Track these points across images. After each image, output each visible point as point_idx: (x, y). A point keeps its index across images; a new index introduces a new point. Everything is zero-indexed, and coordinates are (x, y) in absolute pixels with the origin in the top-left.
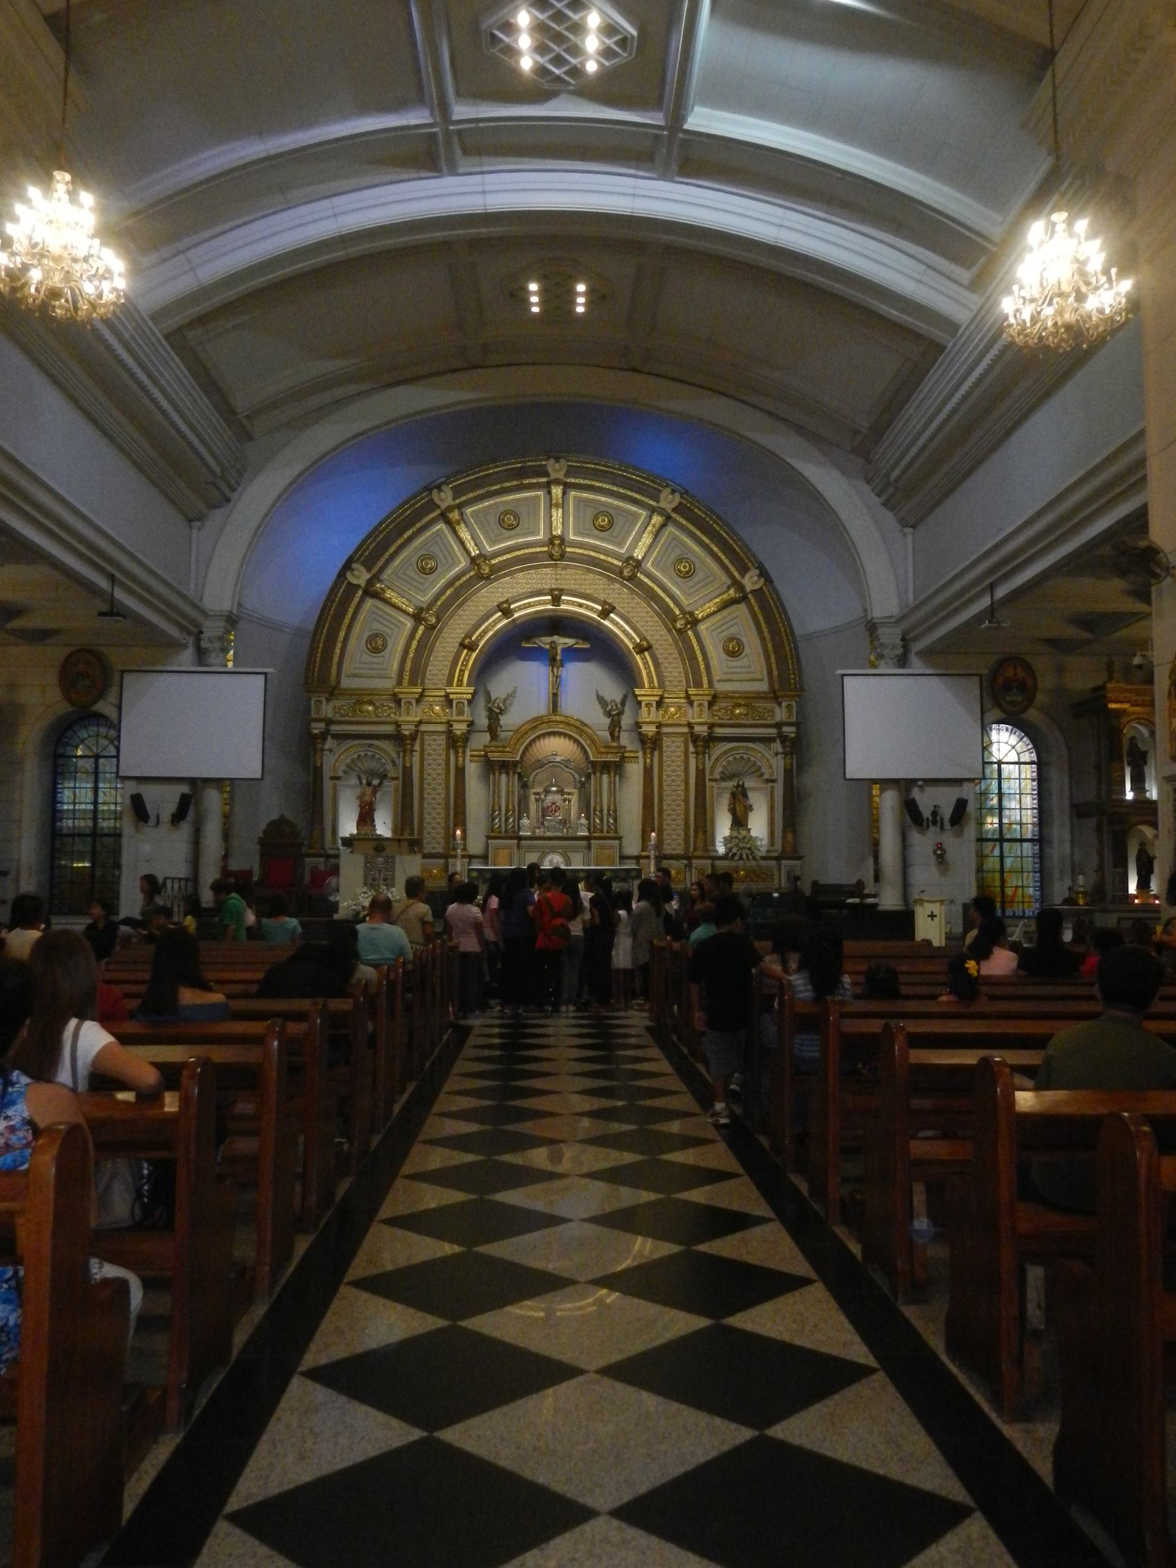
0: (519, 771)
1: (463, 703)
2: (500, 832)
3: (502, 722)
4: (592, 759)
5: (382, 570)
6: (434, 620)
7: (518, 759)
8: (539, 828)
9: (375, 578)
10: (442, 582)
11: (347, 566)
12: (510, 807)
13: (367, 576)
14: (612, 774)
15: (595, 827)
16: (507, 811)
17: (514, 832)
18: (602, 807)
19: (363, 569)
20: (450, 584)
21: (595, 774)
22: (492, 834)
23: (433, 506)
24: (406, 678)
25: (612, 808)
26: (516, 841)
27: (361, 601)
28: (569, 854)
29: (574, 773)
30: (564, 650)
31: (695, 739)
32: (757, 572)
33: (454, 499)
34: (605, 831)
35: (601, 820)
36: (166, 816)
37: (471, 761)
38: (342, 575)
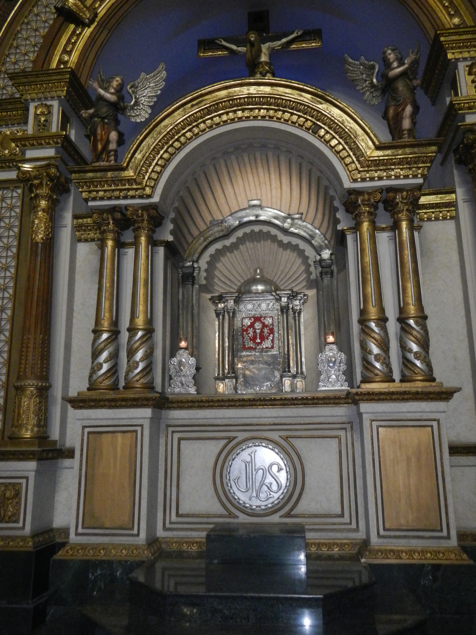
0: (170, 238)
1: (49, 107)
2: (114, 387)
4: (347, 184)
7: (156, 199)
8: (222, 379)
12: (140, 321)
14: (404, 225)
15: (367, 365)
16: (132, 330)
17: (150, 387)
18: (382, 310)
21: (357, 228)
22: (94, 395)
25: (412, 310)
26: (147, 412)
28: (297, 443)
29: (302, 245)
30: (273, 53)
34: (396, 375)
37: (76, 240)
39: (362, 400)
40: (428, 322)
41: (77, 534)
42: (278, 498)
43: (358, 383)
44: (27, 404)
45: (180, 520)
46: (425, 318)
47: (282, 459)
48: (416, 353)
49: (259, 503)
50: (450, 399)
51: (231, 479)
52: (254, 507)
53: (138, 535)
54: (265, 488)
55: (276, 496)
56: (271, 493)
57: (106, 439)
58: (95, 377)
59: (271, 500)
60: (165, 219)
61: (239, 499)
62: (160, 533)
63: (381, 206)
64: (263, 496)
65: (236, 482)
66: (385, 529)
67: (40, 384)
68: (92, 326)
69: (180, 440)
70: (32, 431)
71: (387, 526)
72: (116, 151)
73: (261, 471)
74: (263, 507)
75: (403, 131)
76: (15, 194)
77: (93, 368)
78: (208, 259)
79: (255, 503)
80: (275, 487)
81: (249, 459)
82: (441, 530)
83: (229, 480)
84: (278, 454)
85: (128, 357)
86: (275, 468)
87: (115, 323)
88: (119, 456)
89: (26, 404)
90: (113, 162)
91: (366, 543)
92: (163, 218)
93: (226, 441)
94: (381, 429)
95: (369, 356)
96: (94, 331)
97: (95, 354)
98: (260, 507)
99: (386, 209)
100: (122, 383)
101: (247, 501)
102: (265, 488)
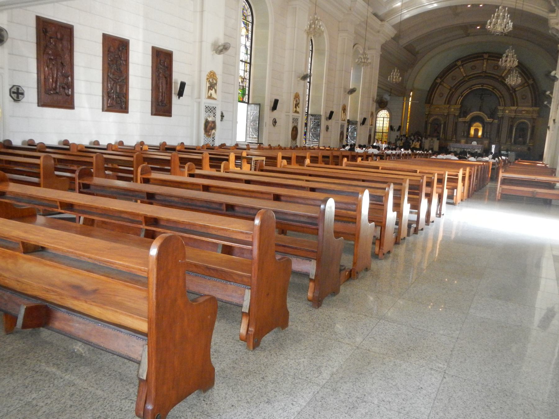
5: (443, 79)
6: (454, 90)
9: (442, 81)
10: (457, 82)
11: (436, 79)
13: (440, 81)
19: (439, 79)
20: (458, 82)
23: (456, 65)
24: (446, 103)
27: (439, 86)
31: (511, 118)
32: (532, 80)
33: (461, 63)
36: (396, 130)
38: (435, 80)
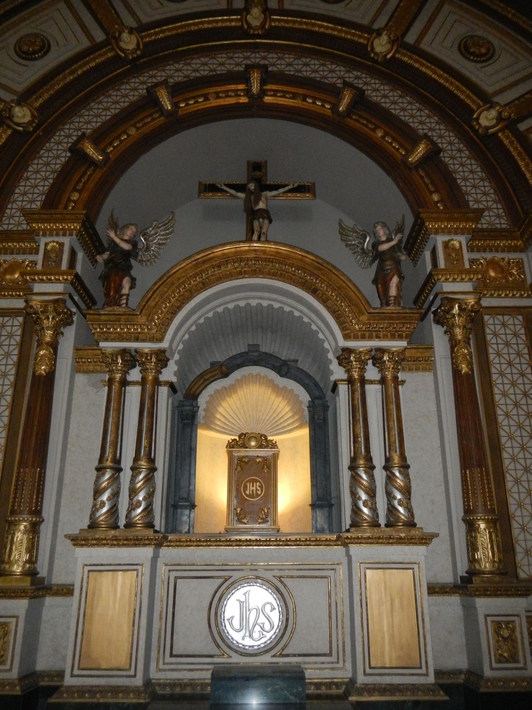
3: (133, 273)
35: (372, 493)
39: (352, 543)
40: (410, 471)
41: (72, 676)
42: (271, 638)
43: (348, 527)
44: (20, 540)
45: (174, 660)
46: (408, 467)
47: (275, 599)
48: (400, 500)
49: (252, 643)
50: (429, 544)
51: (226, 619)
52: (247, 648)
53: (135, 676)
54: (257, 628)
55: (269, 635)
56: (264, 633)
57: (106, 579)
58: (98, 515)
59: (263, 640)
60: (170, 361)
61: (232, 638)
62: (154, 675)
63: (370, 362)
64: (256, 635)
65: (230, 621)
66: (370, 668)
67: (34, 519)
68: (96, 463)
69: (176, 578)
70: (24, 566)
71: (373, 665)
72: (128, 295)
73: (255, 610)
74: (256, 648)
75: (390, 297)
76: (16, 323)
77: (94, 505)
78: (208, 399)
79: (248, 642)
80: (267, 627)
81: (243, 599)
82: (421, 668)
83: (224, 620)
84: (271, 594)
85: (130, 496)
86: (268, 608)
87: (117, 461)
88: (118, 595)
89: (19, 539)
90: (124, 305)
91: (352, 681)
92: (168, 360)
93: (221, 580)
94: (368, 571)
95: (359, 501)
96: (98, 469)
97: (98, 492)
98: (253, 646)
99: (374, 364)
100: (122, 522)
101: (240, 641)
102: (257, 628)
